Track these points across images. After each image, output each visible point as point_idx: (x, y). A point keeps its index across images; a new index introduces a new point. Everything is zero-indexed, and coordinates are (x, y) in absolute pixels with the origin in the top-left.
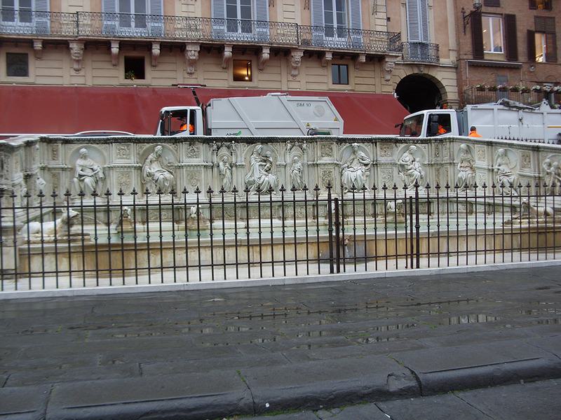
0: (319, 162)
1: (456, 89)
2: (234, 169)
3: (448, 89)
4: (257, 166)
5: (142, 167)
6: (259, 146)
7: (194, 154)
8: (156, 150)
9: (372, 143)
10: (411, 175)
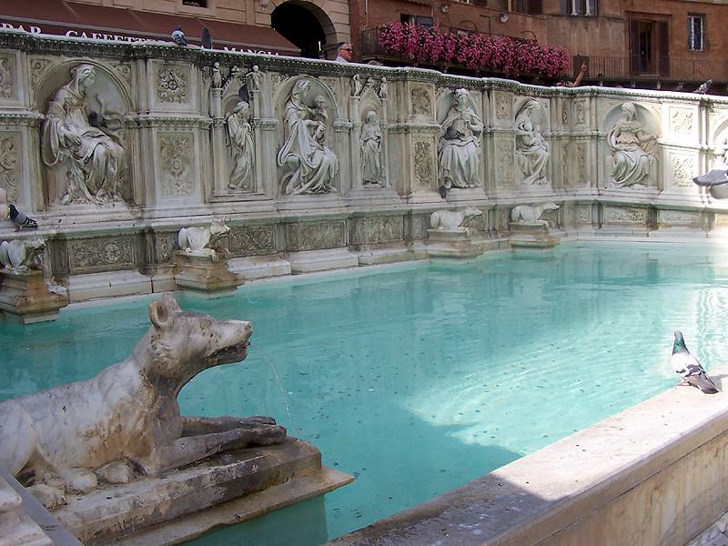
0: (410, 123)
1: (347, 30)
2: (257, 131)
3: (338, 28)
4: (305, 128)
5: (42, 122)
6: (304, 83)
7: (172, 89)
8: (80, 75)
9: (483, 91)
10: (534, 157)
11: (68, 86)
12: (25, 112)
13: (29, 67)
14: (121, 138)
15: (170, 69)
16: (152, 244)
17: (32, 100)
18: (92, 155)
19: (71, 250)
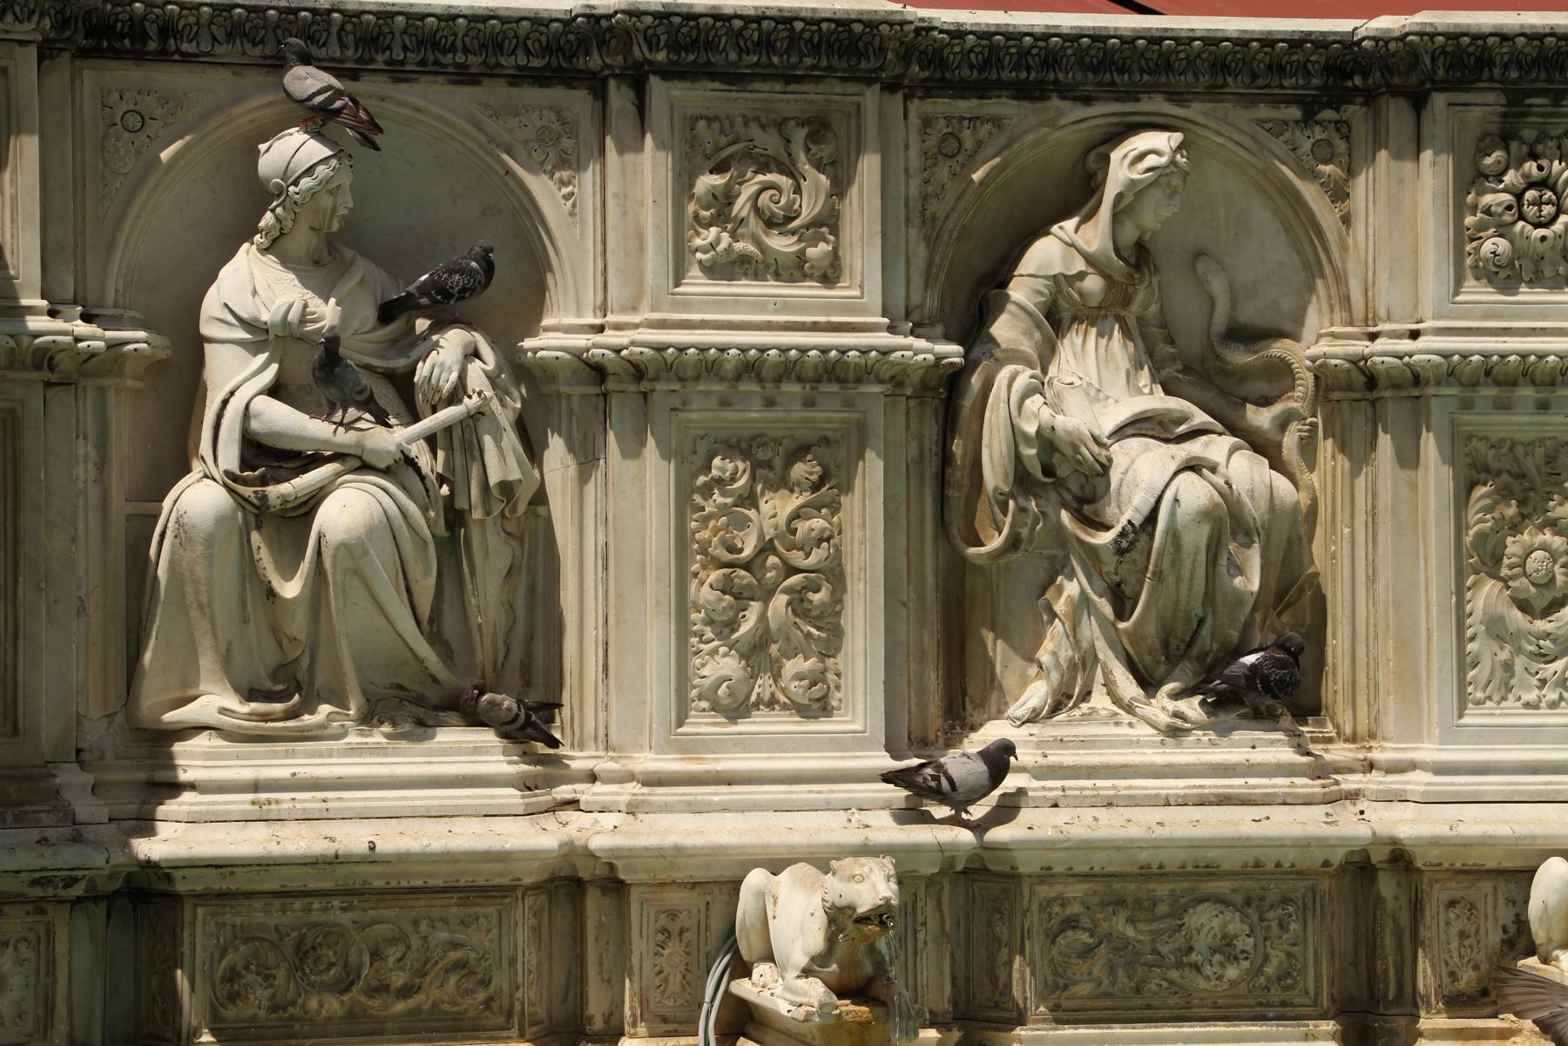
11: (1070, 224)
12: (884, 339)
13: (914, 152)
14: (1290, 441)
15: (1529, 134)
16: (1405, 919)
17: (917, 281)
18: (1152, 518)
19: (1035, 918)
